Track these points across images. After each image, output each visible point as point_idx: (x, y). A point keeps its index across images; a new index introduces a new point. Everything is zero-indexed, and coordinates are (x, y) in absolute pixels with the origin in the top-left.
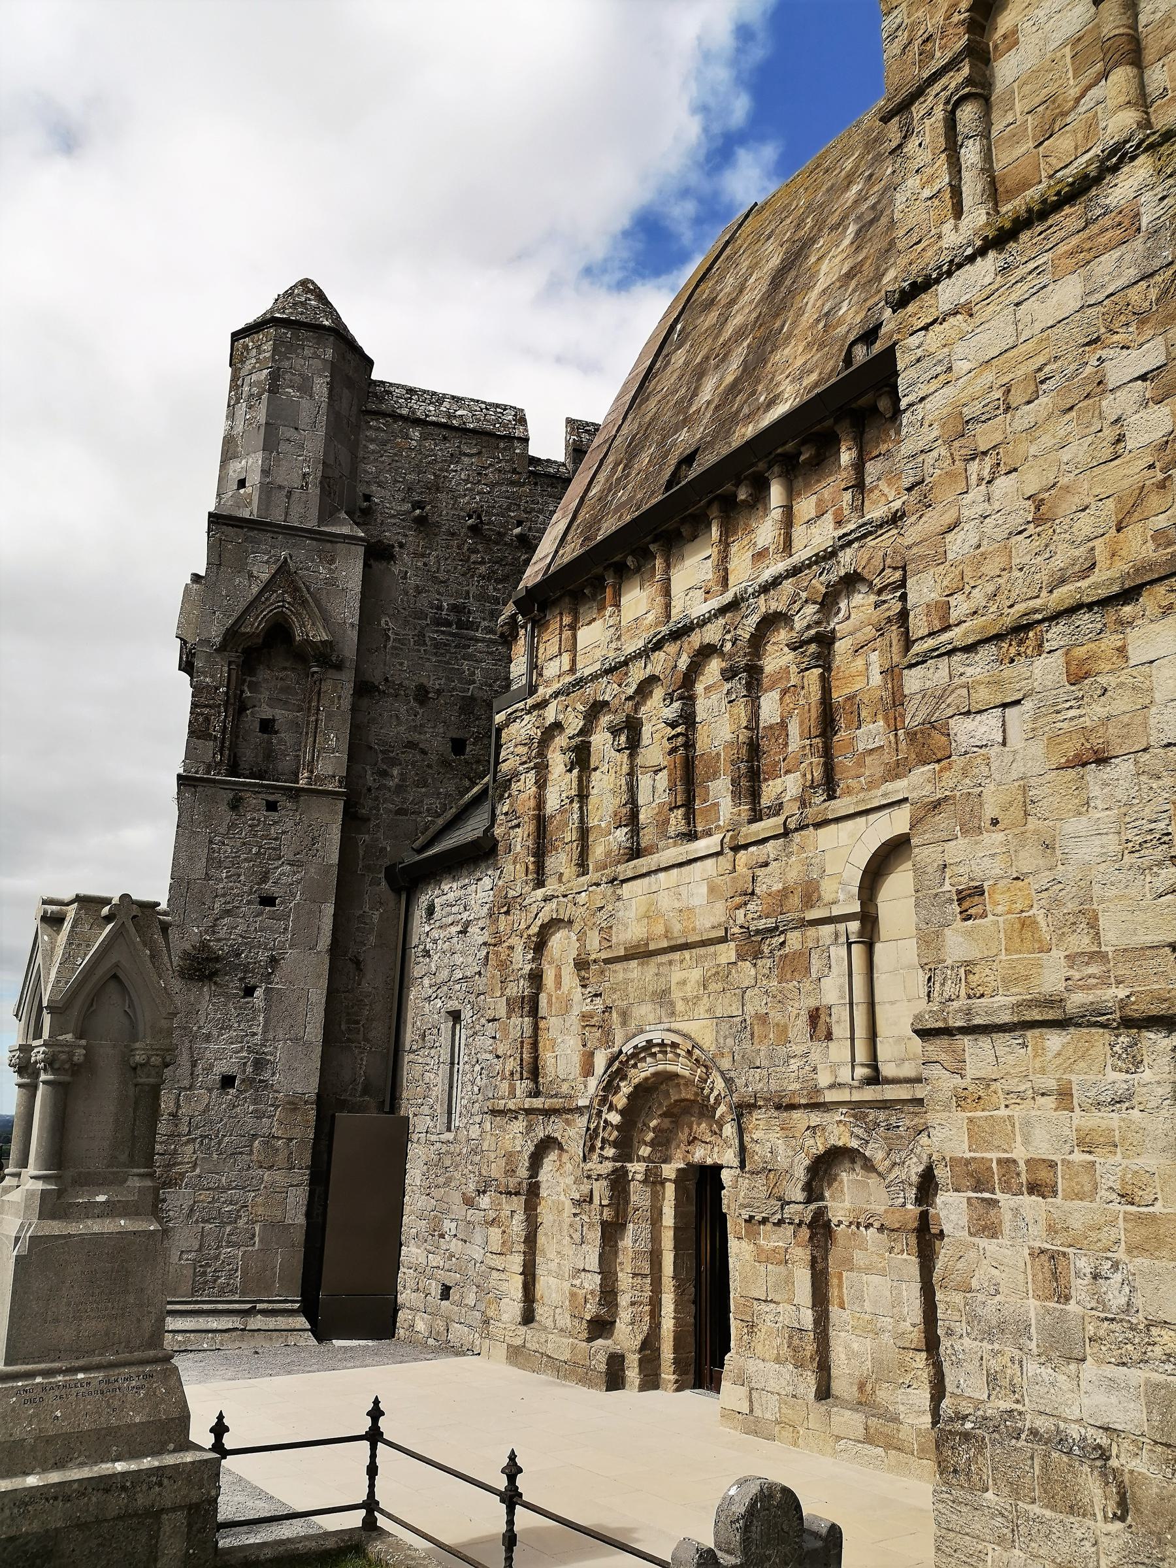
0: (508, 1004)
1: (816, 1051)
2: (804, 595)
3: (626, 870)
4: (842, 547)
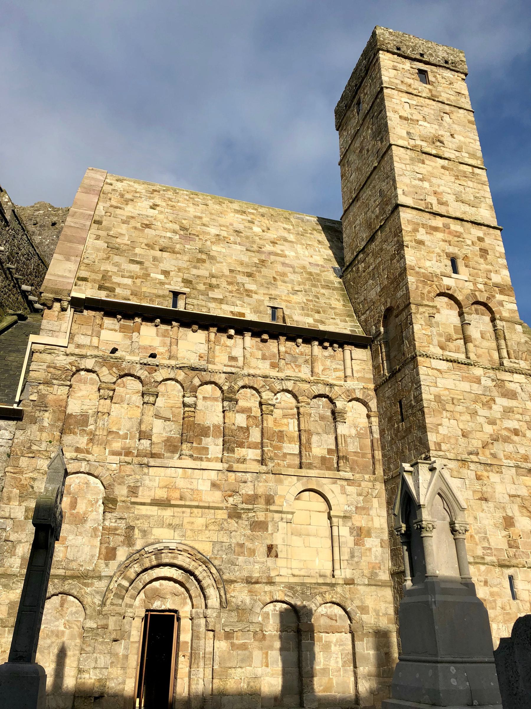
0: (26, 511)
1: (270, 562)
2: (268, 388)
3: (152, 462)
4: (286, 380)
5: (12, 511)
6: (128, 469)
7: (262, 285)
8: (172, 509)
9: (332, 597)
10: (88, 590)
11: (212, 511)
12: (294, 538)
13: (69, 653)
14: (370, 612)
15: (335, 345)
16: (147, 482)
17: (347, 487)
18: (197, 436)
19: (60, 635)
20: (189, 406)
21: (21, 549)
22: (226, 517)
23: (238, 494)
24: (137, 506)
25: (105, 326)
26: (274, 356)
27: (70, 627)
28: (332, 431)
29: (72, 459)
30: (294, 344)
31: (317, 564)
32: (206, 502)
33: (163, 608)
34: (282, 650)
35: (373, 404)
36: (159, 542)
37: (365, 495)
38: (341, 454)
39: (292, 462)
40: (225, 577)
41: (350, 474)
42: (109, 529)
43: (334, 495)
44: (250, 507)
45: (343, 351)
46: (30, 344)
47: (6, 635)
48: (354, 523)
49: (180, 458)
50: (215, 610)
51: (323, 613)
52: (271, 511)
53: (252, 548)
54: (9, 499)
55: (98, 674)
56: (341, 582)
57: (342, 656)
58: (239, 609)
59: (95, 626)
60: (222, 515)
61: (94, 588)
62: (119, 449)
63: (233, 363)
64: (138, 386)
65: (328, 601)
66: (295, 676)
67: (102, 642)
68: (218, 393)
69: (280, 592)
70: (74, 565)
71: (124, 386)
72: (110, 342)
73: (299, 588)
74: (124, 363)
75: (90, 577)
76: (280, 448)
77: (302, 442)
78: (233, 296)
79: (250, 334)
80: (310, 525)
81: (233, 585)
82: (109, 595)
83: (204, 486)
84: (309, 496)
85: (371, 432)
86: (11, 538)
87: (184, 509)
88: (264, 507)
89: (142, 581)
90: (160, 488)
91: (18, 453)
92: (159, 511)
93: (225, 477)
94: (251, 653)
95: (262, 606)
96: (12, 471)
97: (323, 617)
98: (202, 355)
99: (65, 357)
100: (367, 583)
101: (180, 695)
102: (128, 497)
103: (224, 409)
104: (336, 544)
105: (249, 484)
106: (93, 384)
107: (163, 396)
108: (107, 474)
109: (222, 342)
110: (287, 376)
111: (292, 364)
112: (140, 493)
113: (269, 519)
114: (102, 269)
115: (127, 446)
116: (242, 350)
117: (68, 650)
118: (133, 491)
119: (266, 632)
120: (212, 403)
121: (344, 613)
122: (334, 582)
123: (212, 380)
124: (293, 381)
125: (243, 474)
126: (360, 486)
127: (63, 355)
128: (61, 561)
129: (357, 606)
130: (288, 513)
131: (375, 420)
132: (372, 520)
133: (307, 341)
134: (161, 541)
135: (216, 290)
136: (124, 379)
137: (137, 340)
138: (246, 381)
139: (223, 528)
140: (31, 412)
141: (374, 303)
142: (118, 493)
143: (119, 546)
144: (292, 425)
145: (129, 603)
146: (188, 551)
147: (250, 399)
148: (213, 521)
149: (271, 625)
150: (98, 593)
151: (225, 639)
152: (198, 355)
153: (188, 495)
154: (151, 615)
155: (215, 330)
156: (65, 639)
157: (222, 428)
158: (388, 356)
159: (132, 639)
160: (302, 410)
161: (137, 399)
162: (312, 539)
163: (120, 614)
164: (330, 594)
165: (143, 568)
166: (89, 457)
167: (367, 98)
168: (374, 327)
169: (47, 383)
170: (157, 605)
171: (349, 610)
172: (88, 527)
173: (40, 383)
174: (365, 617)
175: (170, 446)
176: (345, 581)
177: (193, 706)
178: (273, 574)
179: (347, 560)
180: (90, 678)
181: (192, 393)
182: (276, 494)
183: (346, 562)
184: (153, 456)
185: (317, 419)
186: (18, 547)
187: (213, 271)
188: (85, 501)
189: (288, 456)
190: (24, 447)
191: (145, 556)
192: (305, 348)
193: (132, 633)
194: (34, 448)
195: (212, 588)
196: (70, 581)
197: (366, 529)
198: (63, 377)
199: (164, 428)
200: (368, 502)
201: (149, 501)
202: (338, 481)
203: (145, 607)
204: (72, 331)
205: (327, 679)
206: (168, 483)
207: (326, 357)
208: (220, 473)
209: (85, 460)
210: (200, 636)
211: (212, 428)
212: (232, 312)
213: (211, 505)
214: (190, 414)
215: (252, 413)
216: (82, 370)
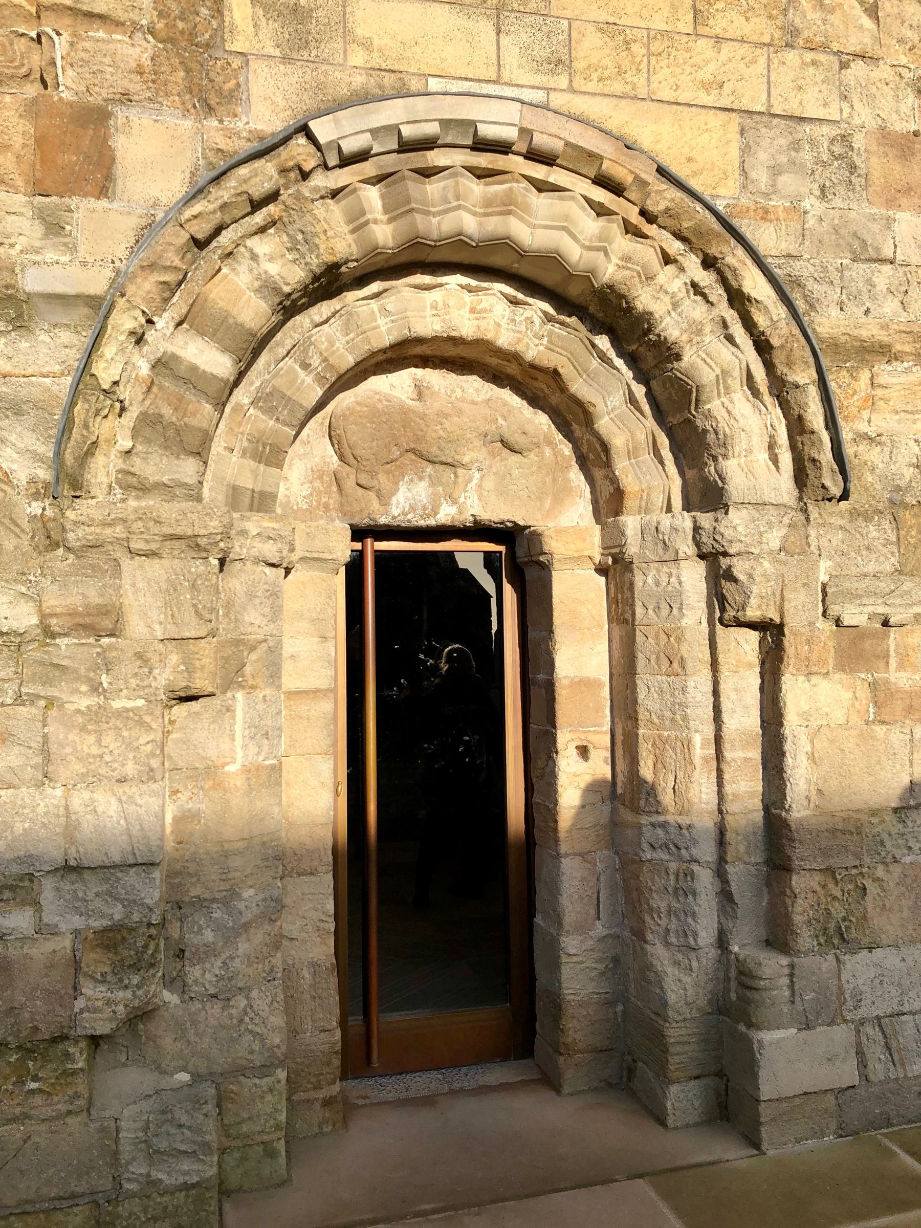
33: (446, 515)
55: (98, 903)
58: (906, 506)
81: (865, 375)
82: (103, 428)
89: (315, 361)
134: (415, 85)
139: (795, 32)
143: (126, 98)
145: (247, 482)
146: (592, 156)
151: (841, 667)
154: (380, 556)
159: (290, 681)
165: (315, 263)
177: (672, 998)
180: (44, 930)
191: (322, 181)
193: (289, 648)
203: (344, 513)
210: (684, 650)
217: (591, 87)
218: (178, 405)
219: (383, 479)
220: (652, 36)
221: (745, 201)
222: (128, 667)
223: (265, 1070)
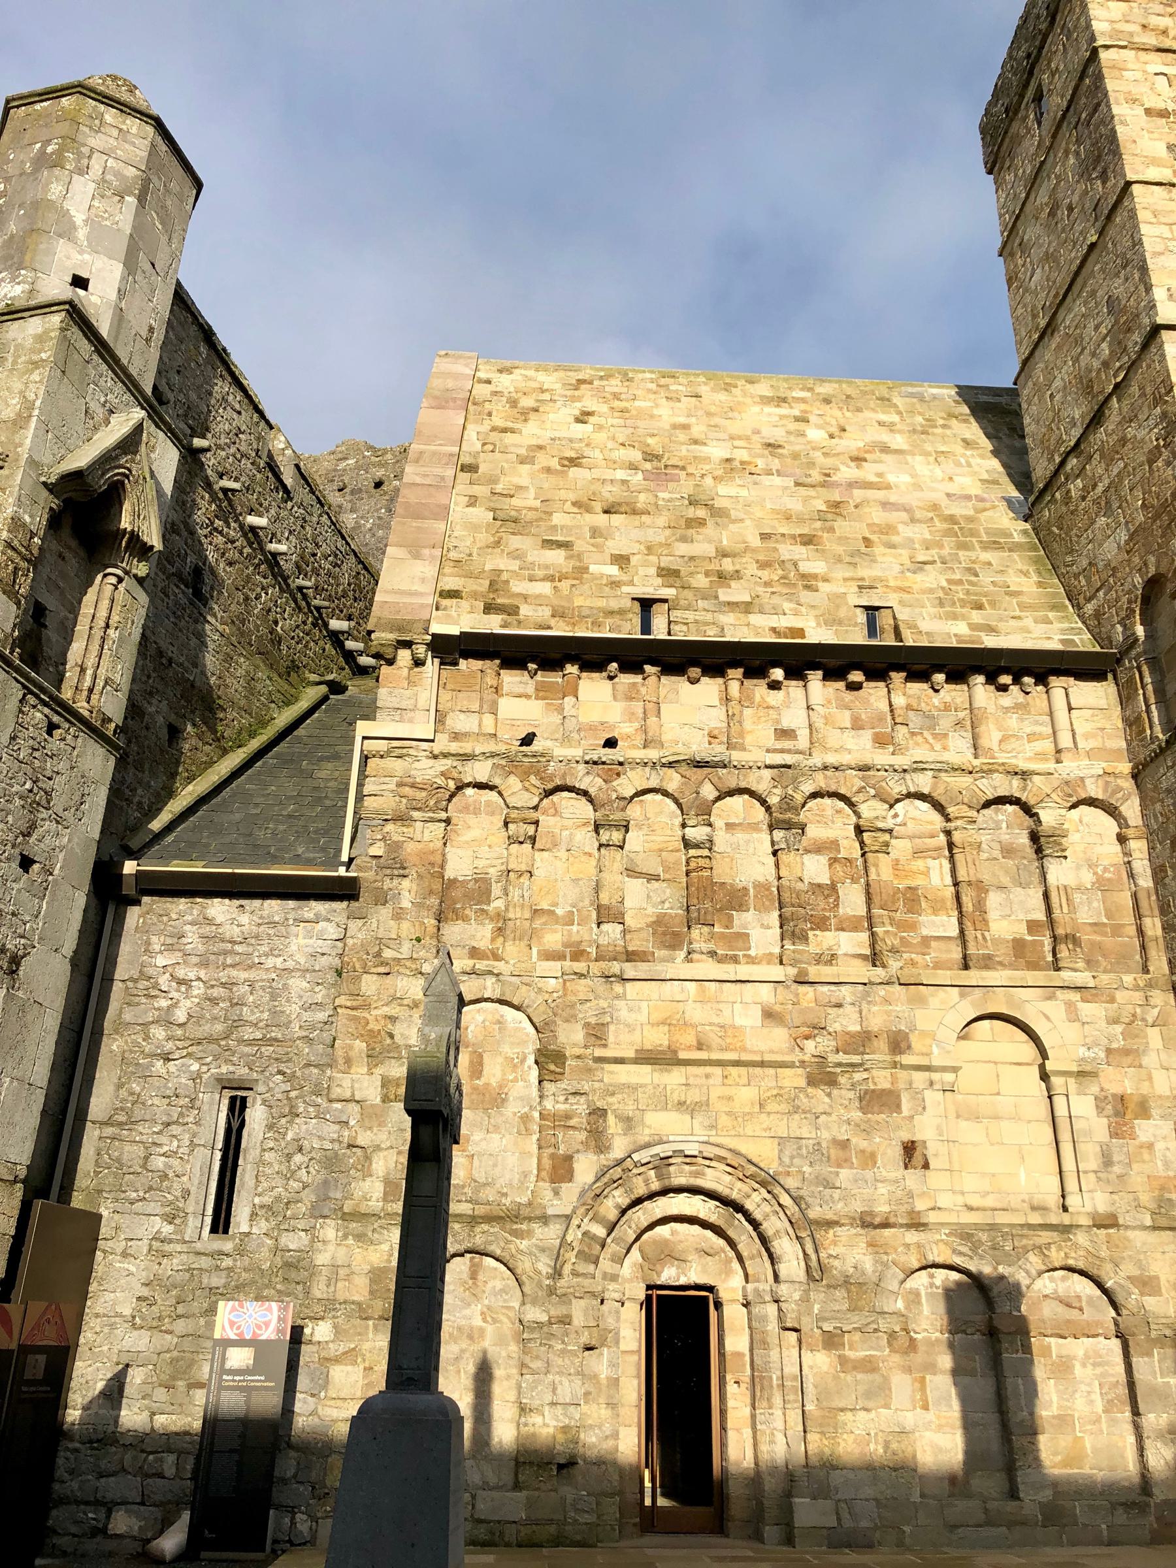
0: (383, 1086)
1: (912, 1178)
2: (872, 792)
3: (630, 970)
4: (915, 770)
5: (356, 1085)
6: (582, 986)
7: (839, 560)
8: (683, 1069)
9: (1066, 1255)
10: (524, 1244)
11: (771, 1071)
12: (963, 1124)
13: (498, 1373)
14: (1163, 1290)
15: (1027, 680)
16: (624, 1014)
17: (1080, 1005)
18: (721, 909)
19: (476, 1336)
20: (697, 846)
21: (381, 1163)
22: (802, 1082)
23: (825, 1032)
24: (608, 1067)
25: (506, 689)
26: (881, 719)
27: (495, 1321)
28: (1036, 878)
29: (465, 973)
30: (925, 686)
31: (1023, 1183)
32: (755, 1052)
33: (683, 1281)
34: (957, 1372)
35: (1132, 809)
36: (661, 1142)
37: (1127, 1020)
38: (1060, 931)
39: (945, 956)
40: (814, 1213)
41: (1087, 974)
42: (554, 1117)
43: (1049, 1025)
44: (856, 1059)
45: (1047, 692)
46: (358, 740)
47: (371, 1335)
48: (1106, 1086)
49: (688, 959)
50: (797, 1286)
51: (1047, 1292)
52: (903, 1067)
53: (869, 1150)
54: (348, 1061)
55: (561, 1417)
56: (1085, 1221)
57: (1101, 1389)
59: (544, 1318)
60: (794, 1079)
61: (534, 1240)
62: (559, 947)
63: (787, 744)
64: (584, 810)
65: (1057, 1265)
66: (993, 1432)
67: (564, 1352)
68: (759, 813)
69: (942, 1246)
70: (489, 1194)
71: (556, 813)
72: (519, 723)
73: (984, 1237)
74: (552, 764)
75: (525, 1218)
76: (913, 927)
77: (964, 909)
78: (773, 593)
79: (820, 674)
80: (998, 1094)
81: (831, 1232)
82: (567, 1255)
83: (748, 1018)
84: (992, 1029)
85: (1131, 875)
86: (360, 1141)
87: (708, 1069)
88: (888, 1058)
89: (633, 1226)
90: (653, 1025)
91: (357, 966)
92: (656, 1075)
93: (791, 997)
94: (886, 1379)
95: (902, 1276)
96: (349, 1004)
97: (1049, 1301)
98: (716, 732)
99: (431, 762)
100: (1148, 1222)
101: (738, 1464)
102: (586, 1047)
103: (776, 847)
104: (1065, 1136)
105: (848, 1009)
106: (493, 814)
107: (639, 827)
108: (540, 1000)
109: (758, 698)
110: (915, 762)
111: (926, 734)
112: (611, 1039)
113: (901, 1085)
114: (488, 567)
115: (575, 938)
116: (804, 712)
117: (494, 1366)
118: (597, 1033)
119: (916, 1333)
120: (746, 836)
121: (1099, 1292)
122: (1067, 1223)
123: (743, 785)
124: (930, 773)
125: (833, 988)
126: (1112, 1000)
127: (428, 757)
128: (463, 1187)
129: (1129, 1277)
130: (944, 1069)
131: (1138, 847)
132: (1150, 1078)
133: (957, 676)
134: (665, 1139)
135: (733, 584)
136: (555, 798)
137: (573, 712)
138: (820, 781)
139: (798, 1107)
140: (376, 881)
141: (1114, 569)
142: (565, 1041)
143: (578, 1151)
144: (937, 871)
145: (609, 1270)
146: (725, 1159)
147: (833, 822)
148: (775, 1092)
149: (928, 1318)
150: (543, 1250)
152: (706, 732)
153: (715, 1041)
154: (658, 1296)
155: (738, 673)
156: (487, 1343)
157: (774, 889)
158: (1160, 692)
159: (623, 1346)
160: (957, 837)
161: (586, 839)
162: (1004, 1124)
163: (593, 1294)
164: (1060, 1248)
165: (633, 1197)
166: (499, 966)
167: (1059, 82)
168: (1119, 628)
169: (401, 818)
170: (669, 1275)
171: (1109, 1285)
172: (511, 1115)
173: (386, 820)
174: (1150, 1302)
175: (664, 934)
176: (1093, 1219)
178: (920, 1205)
179: (1095, 1172)
180: (546, 1425)
181: (700, 818)
182: (913, 1028)
183: (1092, 1176)
184: (631, 956)
185: (997, 853)
186: (375, 1159)
187: (725, 542)
188: (500, 1060)
189: (933, 944)
190: (368, 954)
191: (635, 1171)
192: (954, 693)
193: (622, 1333)
194: (388, 954)
195: (786, 1239)
196: (485, 1227)
197: (1135, 1099)
198: (432, 803)
199: (648, 897)
200: (1137, 1036)
201: (631, 1054)
202: (1059, 992)
203: (644, 1281)
204: (440, 707)
205: (1070, 1438)
206: (668, 1014)
207: (1007, 710)
208: (780, 987)
209: (490, 973)
211: (752, 891)
212: (774, 630)
213: (768, 1057)
214: (701, 862)
215: (839, 852)
216: (468, 785)
217: (725, 1133)
218: (590, 1247)
219: (658, 1267)
220: (745, 1114)
221: (781, 1169)
222: (573, 1336)
223: (612, 1495)
